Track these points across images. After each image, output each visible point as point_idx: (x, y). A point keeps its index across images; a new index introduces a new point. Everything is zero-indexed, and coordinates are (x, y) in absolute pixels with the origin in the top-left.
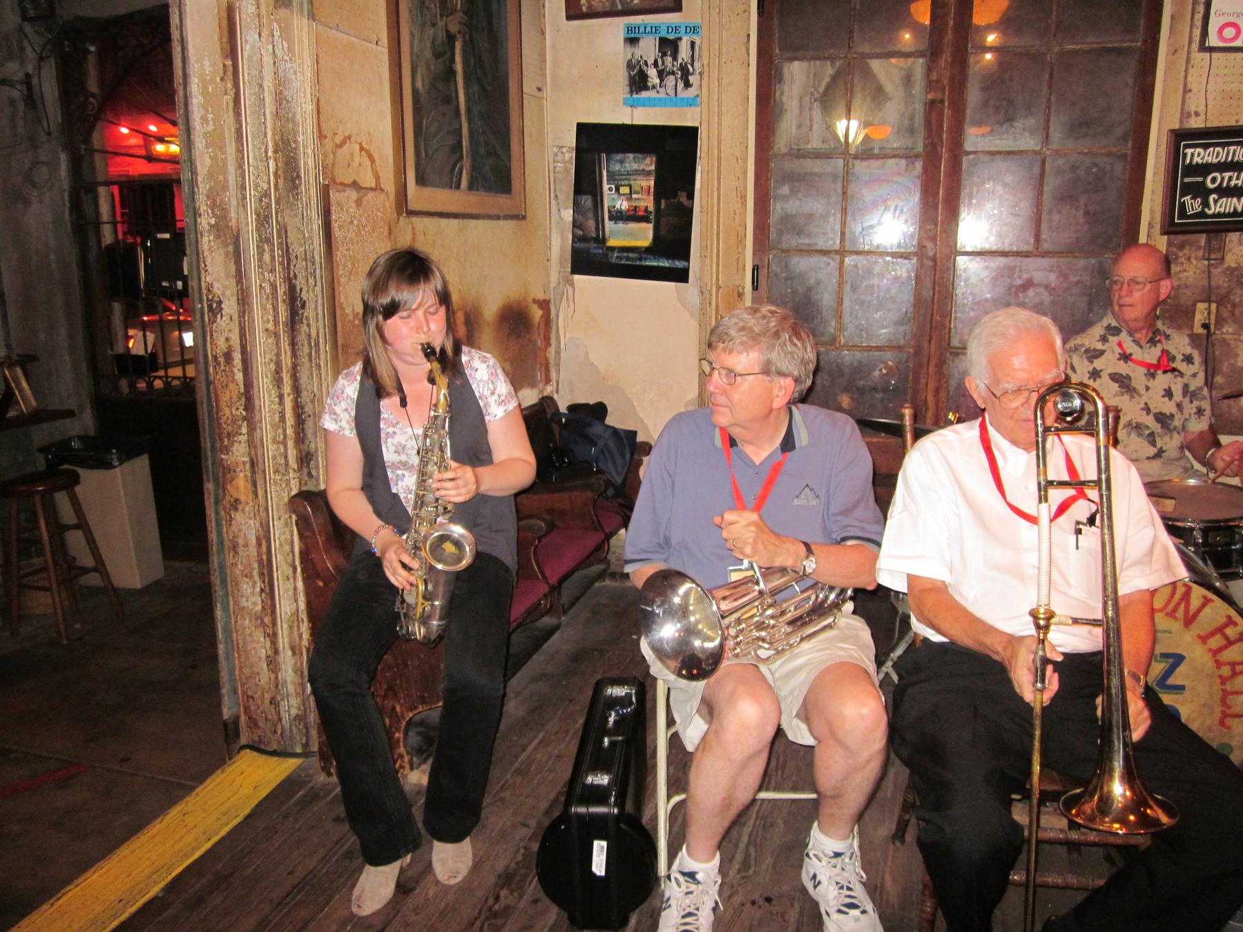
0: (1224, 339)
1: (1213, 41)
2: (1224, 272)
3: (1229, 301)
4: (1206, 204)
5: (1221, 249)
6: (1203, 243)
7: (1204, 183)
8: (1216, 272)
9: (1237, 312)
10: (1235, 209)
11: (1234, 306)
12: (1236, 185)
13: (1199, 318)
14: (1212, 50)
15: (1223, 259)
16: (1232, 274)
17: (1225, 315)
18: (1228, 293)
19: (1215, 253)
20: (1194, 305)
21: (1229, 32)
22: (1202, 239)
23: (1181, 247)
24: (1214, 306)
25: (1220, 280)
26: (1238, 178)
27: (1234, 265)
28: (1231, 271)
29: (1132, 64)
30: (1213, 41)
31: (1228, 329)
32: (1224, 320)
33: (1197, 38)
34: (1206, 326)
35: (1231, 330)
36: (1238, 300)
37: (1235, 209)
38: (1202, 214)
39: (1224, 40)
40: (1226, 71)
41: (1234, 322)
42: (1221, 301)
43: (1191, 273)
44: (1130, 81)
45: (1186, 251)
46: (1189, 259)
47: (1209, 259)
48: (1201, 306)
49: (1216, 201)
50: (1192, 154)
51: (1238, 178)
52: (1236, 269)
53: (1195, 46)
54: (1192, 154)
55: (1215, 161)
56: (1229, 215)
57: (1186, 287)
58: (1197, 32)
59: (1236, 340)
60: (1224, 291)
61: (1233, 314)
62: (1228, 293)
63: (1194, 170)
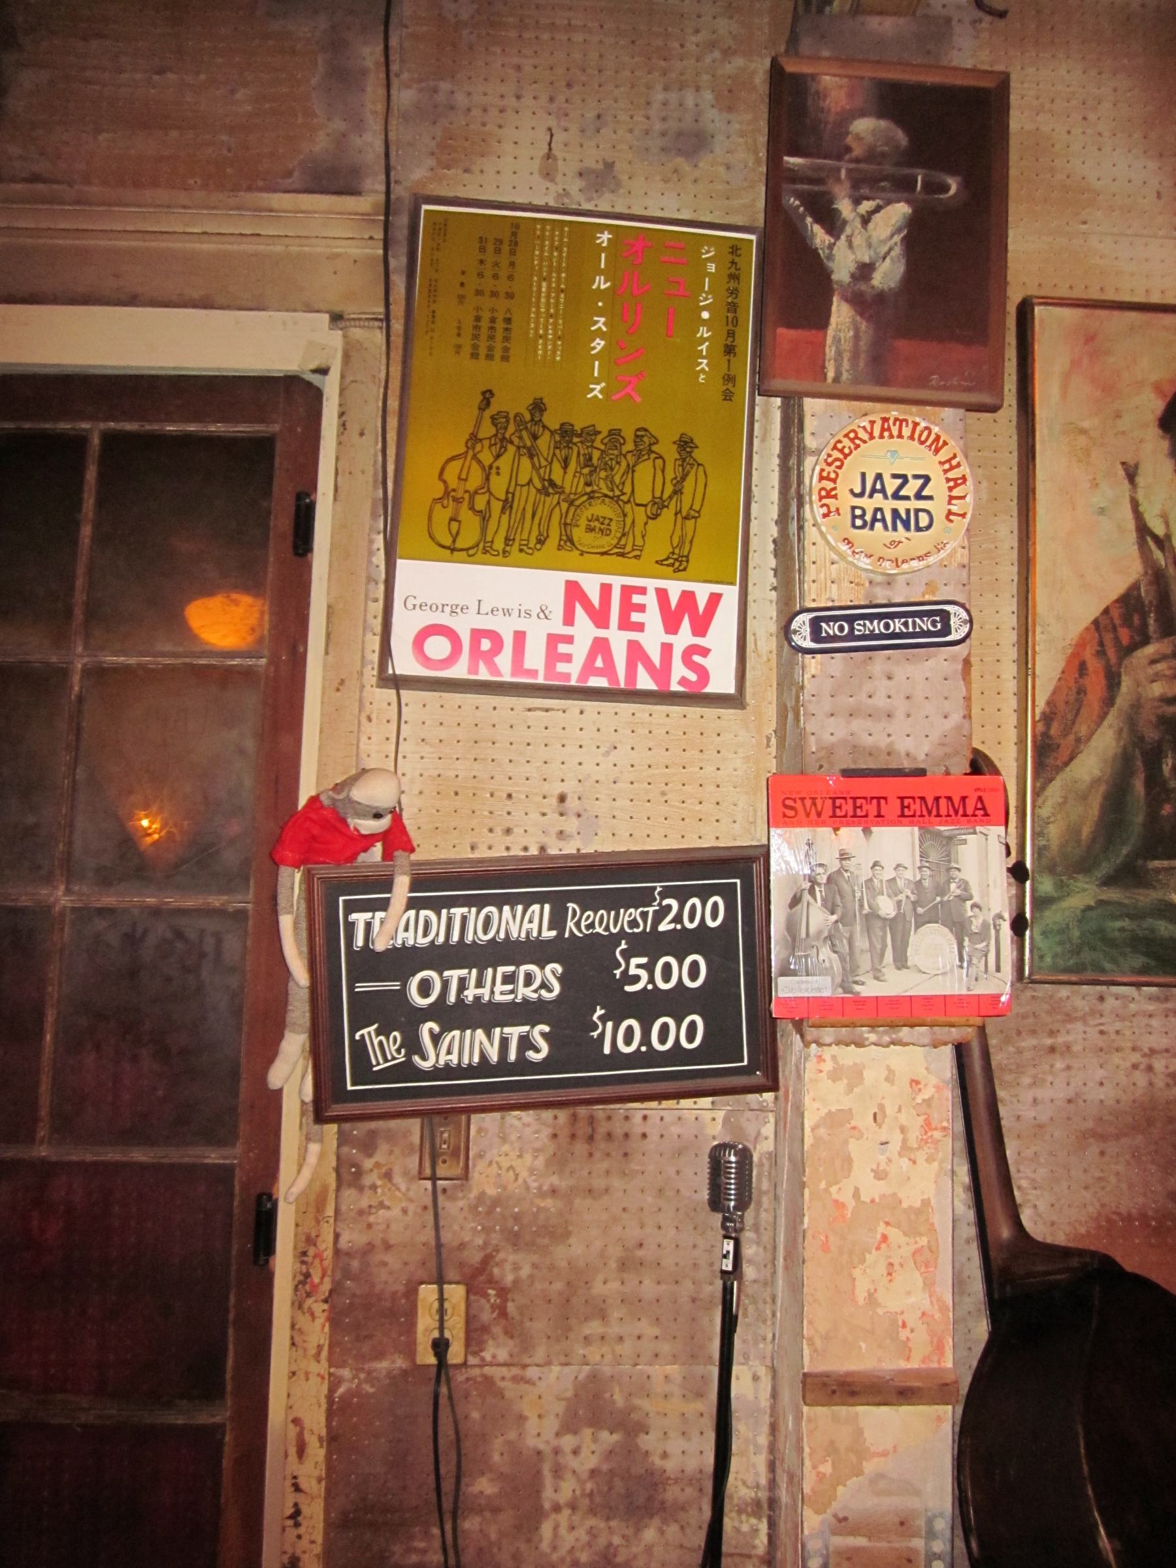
0: (488, 1381)
1: (404, 663)
2: (473, 1208)
3: (491, 1282)
4: (412, 1045)
5: (461, 1152)
6: (416, 1139)
7: (403, 992)
8: (452, 1208)
9: (511, 1307)
10: (483, 1055)
11: (503, 1292)
12: (477, 999)
13: (426, 1325)
14: (398, 683)
15: (466, 1176)
16: (490, 1211)
17: (486, 1316)
18: (487, 1260)
19: (444, 1160)
20: (411, 1292)
21: (438, 647)
22: (415, 1125)
23: (368, 1145)
24: (456, 1293)
25: (463, 1228)
26: (480, 984)
27: (492, 1191)
28: (488, 1207)
29: (251, 701)
30: (404, 663)
31: (497, 1350)
32: (485, 1329)
33: (375, 658)
34: (440, 1346)
35: (503, 1355)
36: (509, 1278)
37: (483, 1055)
38: (406, 1070)
39: (426, 661)
40: (442, 733)
41: (509, 1334)
42: (477, 1279)
43: (396, 1212)
44: (250, 744)
45: (380, 1156)
46: (388, 1176)
47: (434, 1178)
48: (427, 1293)
49: (436, 1039)
50: (368, 925)
51: (480, 984)
52: (496, 1202)
53: (371, 674)
54: (368, 925)
55: (423, 942)
56: (471, 1072)
57: (388, 1247)
58: (375, 643)
59: (516, 1379)
60: (476, 1258)
61: (503, 1313)
62: (487, 1260)
63: (370, 963)
